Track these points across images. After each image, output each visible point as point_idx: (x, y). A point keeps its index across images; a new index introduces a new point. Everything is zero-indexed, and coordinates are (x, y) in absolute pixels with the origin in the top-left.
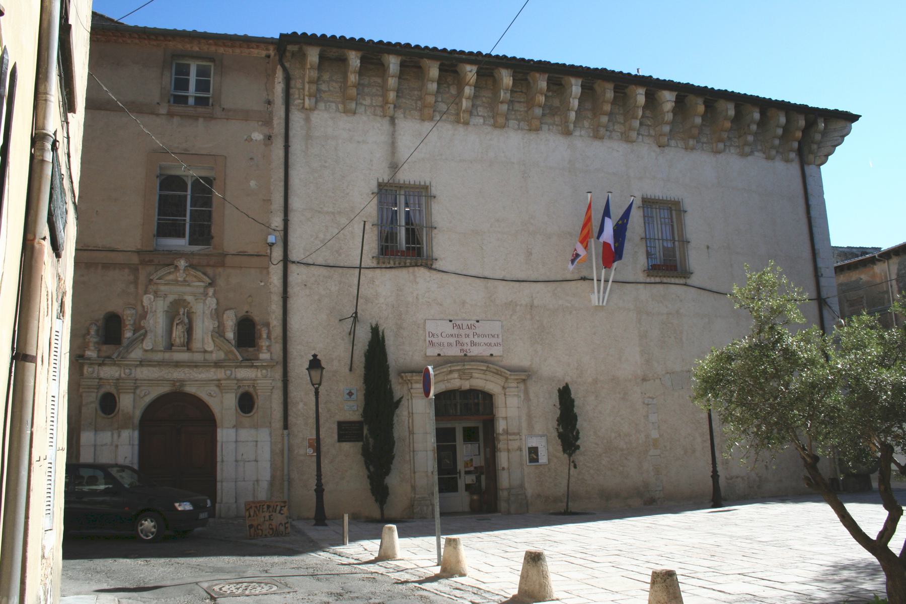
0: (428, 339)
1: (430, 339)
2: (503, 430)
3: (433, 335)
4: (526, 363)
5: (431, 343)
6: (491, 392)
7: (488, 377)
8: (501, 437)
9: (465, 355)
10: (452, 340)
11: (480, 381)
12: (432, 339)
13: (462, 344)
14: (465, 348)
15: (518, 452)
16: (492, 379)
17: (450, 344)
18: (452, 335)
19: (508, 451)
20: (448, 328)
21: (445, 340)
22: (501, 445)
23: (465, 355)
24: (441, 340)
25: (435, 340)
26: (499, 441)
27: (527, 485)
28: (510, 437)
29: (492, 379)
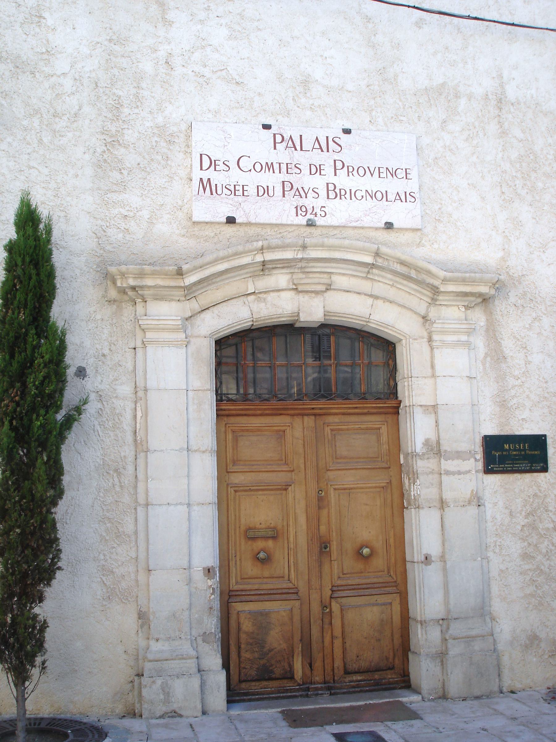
0: (197, 174)
1: (205, 175)
2: (427, 443)
3: (213, 163)
4: (488, 255)
5: (206, 185)
6: (389, 333)
7: (379, 289)
8: (421, 465)
9: (311, 224)
10: (272, 180)
11: (351, 303)
12: (210, 174)
13: (301, 193)
14: (309, 202)
15: (473, 510)
16: (391, 293)
17: (264, 191)
18: (270, 167)
19: (442, 504)
20: (261, 148)
21: (252, 180)
22: (421, 489)
23: (311, 224)
24: (235, 177)
25: (218, 178)
26: (414, 476)
27: (497, 606)
28: (447, 465)
29: (391, 293)
